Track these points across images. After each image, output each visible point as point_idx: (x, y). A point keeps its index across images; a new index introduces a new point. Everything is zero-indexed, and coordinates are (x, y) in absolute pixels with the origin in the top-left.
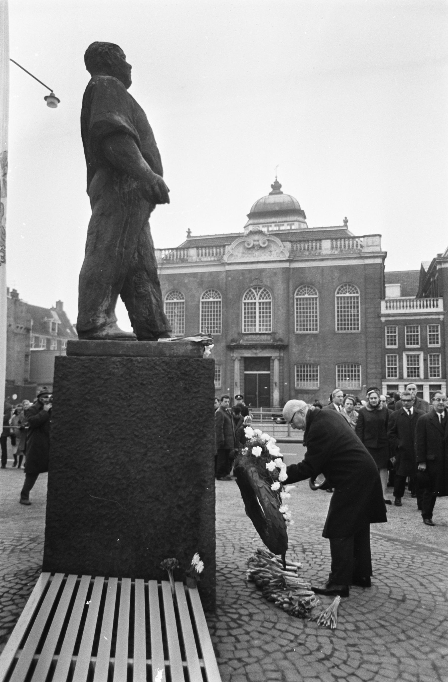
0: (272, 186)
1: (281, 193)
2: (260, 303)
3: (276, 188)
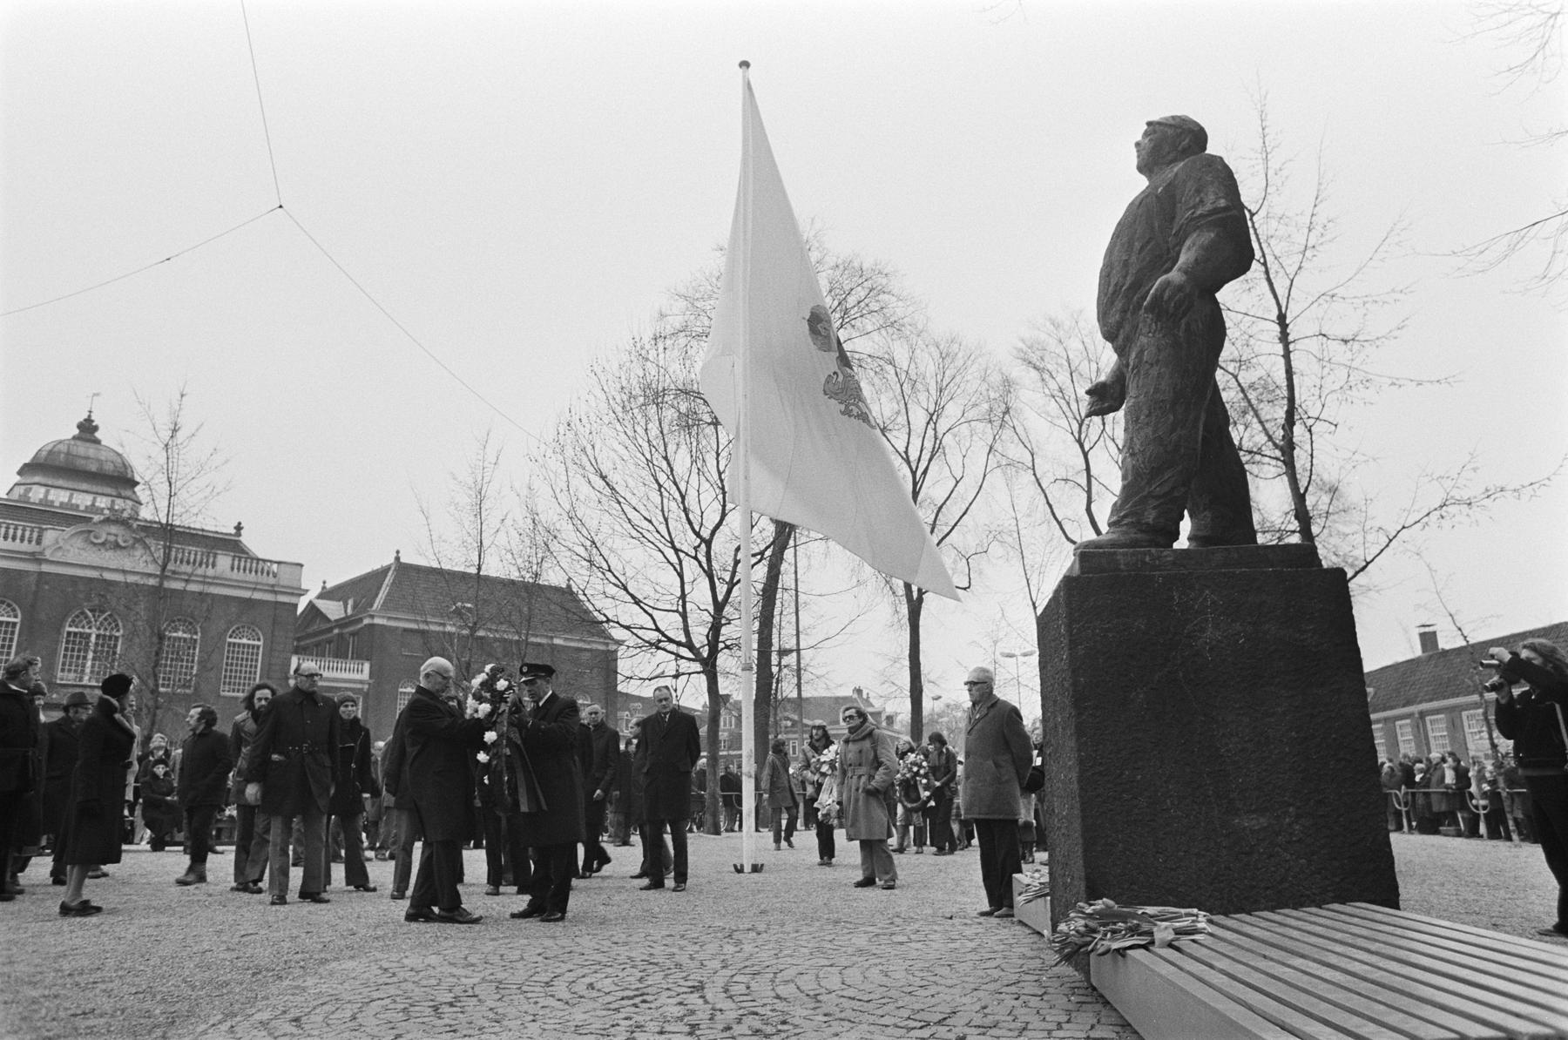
0: (80, 426)
1: (98, 442)
2: (98, 636)
3: (87, 429)
